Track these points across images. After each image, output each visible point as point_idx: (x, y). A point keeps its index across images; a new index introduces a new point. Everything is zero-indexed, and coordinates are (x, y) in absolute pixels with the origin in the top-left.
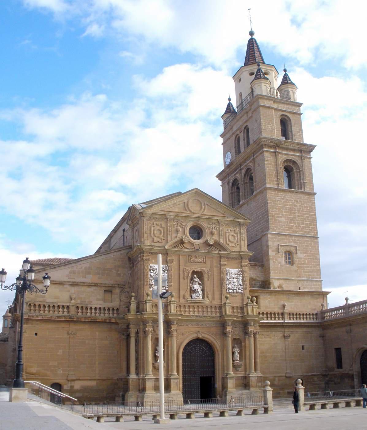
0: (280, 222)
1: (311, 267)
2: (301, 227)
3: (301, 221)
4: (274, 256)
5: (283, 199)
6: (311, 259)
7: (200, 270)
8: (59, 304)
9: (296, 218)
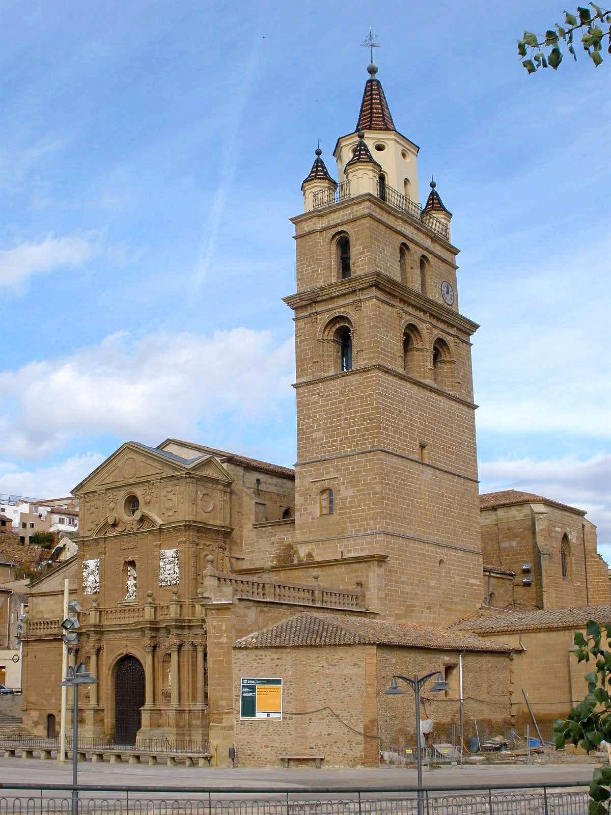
0: (314, 440)
1: (364, 511)
2: (348, 439)
3: (350, 427)
4: (301, 505)
5: (321, 396)
6: (364, 495)
7: (132, 559)
8: (51, 620)
9: (341, 425)
